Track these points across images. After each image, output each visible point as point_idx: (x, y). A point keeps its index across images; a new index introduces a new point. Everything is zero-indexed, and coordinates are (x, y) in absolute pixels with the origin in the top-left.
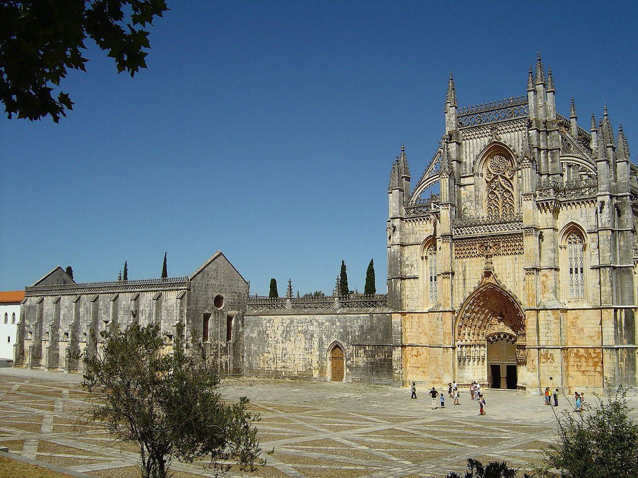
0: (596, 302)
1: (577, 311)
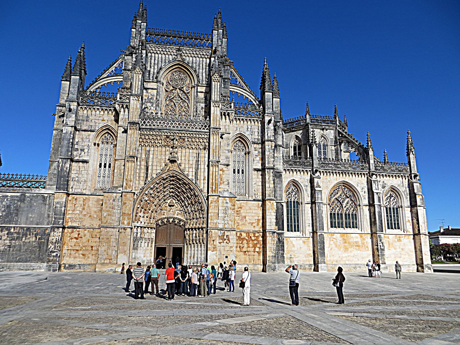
0: (256, 196)
1: (241, 202)
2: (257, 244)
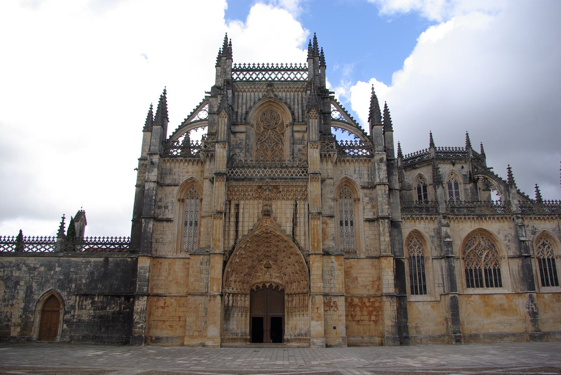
0: (370, 252)
1: (351, 260)
2: (372, 311)
